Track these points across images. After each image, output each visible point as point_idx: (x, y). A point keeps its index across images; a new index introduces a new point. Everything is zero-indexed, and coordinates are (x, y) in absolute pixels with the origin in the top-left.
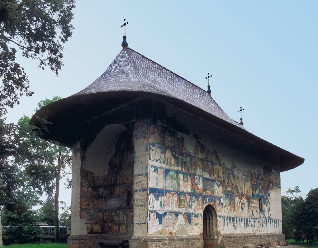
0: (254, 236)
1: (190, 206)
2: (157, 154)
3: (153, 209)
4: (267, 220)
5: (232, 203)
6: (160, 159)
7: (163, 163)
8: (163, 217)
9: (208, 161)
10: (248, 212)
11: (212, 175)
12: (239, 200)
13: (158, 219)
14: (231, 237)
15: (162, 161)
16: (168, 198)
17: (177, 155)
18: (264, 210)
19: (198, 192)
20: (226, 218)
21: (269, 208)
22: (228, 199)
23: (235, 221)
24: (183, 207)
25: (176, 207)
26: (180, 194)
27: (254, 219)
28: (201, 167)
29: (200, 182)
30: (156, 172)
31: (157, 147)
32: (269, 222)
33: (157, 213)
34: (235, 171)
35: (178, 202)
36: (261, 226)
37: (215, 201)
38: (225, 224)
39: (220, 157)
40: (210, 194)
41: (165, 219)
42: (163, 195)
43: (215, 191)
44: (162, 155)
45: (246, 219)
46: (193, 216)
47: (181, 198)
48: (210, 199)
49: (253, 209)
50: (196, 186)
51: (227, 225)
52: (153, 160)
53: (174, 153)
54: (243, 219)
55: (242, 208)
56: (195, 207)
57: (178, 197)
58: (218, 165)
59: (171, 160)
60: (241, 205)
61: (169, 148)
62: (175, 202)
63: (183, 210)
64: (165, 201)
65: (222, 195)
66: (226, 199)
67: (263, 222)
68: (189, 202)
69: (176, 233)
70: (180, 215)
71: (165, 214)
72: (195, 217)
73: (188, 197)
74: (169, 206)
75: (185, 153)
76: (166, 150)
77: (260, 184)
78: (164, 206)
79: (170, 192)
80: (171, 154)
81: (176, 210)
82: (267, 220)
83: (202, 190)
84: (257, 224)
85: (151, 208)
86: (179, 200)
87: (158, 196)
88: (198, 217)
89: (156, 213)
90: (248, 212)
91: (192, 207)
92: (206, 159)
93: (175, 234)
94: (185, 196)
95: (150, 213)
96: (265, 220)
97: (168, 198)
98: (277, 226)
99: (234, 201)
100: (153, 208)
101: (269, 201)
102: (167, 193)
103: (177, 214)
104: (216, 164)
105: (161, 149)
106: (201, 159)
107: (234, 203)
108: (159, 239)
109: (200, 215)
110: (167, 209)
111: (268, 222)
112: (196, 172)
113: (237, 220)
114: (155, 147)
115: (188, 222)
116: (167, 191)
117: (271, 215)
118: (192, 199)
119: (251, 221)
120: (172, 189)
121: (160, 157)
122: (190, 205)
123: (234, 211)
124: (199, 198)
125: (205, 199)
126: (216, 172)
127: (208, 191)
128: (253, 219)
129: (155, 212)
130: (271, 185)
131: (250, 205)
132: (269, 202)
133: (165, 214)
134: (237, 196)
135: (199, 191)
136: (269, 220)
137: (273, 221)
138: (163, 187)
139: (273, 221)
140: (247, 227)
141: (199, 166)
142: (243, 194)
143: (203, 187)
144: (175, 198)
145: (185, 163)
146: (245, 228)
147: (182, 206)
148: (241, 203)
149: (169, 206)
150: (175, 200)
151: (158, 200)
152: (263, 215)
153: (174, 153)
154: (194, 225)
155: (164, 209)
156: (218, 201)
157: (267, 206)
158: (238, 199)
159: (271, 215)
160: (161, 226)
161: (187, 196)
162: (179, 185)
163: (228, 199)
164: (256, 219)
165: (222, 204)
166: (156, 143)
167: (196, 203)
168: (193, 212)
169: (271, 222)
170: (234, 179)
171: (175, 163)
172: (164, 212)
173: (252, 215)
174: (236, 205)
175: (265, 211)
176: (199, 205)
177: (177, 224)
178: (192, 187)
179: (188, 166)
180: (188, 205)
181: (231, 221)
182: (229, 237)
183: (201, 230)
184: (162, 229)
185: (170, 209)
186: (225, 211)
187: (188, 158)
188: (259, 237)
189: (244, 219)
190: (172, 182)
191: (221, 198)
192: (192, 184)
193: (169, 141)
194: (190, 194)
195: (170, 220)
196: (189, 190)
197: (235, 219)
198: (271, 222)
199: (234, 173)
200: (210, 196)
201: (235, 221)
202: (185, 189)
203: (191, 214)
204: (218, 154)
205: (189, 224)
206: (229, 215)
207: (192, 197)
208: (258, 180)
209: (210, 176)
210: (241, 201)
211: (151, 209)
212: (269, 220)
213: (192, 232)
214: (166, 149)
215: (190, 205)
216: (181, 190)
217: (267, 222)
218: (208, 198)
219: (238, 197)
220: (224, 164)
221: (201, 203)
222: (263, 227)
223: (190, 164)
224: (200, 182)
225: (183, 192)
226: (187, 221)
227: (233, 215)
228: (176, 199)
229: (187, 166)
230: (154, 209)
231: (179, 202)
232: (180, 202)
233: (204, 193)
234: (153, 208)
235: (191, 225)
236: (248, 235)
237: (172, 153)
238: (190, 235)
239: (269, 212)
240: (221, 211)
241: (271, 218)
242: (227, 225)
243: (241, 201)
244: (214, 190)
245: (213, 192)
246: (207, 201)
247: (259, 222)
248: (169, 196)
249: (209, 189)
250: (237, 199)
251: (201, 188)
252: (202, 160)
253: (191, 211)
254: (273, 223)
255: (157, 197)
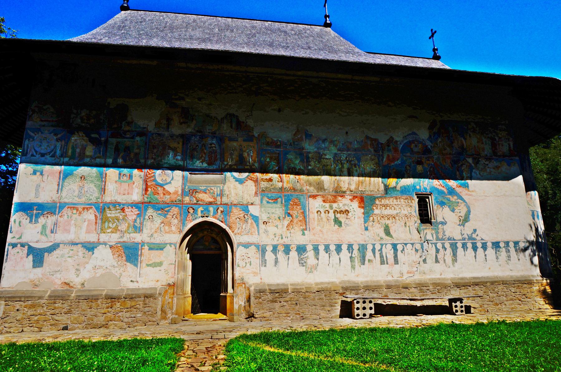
0: (389, 287)
1: (139, 229)
2: (45, 145)
3: (19, 241)
4: (459, 245)
5: (294, 213)
6: (52, 151)
7: (62, 156)
8: (46, 254)
9: (203, 137)
10: (366, 229)
11: (218, 162)
12: (327, 205)
13: (31, 257)
14: (285, 291)
15: (58, 153)
16: (66, 217)
17: (103, 139)
18: (439, 219)
19: (167, 198)
20: (269, 248)
21: (463, 214)
22: (279, 205)
23: (310, 254)
24: (112, 232)
25: (88, 232)
26: (102, 209)
27: (394, 246)
28: (180, 150)
29: (173, 178)
30: (38, 173)
31: (46, 132)
32: (470, 250)
33: (30, 247)
34: (309, 147)
35: (96, 223)
36: (431, 260)
37: (226, 213)
38: (264, 263)
39: (250, 123)
40: (212, 200)
41: (48, 258)
42: (53, 213)
43: (227, 192)
44: (59, 144)
45: (356, 247)
46: (146, 247)
47: (109, 215)
48: (209, 211)
49: (388, 222)
50: (159, 189)
51: (276, 262)
52: (32, 155)
53: (93, 136)
54: (344, 247)
55: (340, 223)
56: (153, 231)
57: (97, 214)
58: (240, 139)
59: (84, 148)
60: (331, 215)
61: (79, 129)
62: (86, 223)
63: (114, 238)
64: (55, 224)
65: (257, 200)
66: (269, 205)
67: (437, 251)
68: (135, 221)
69: (83, 284)
70: (101, 247)
71: (55, 247)
72: (150, 249)
73: (132, 214)
74: (68, 231)
75: (129, 131)
76: (74, 134)
77: (420, 163)
78: (52, 232)
79: (73, 207)
80: (85, 138)
81: (92, 238)
82: (459, 245)
83: (180, 192)
84: (408, 257)
85: (14, 237)
86: (102, 219)
87: (37, 216)
88: (162, 249)
89: (27, 247)
90: (366, 229)
91: (145, 230)
92: (199, 134)
93: (79, 287)
94: (123, 210)
95: (11, 247)
96: (447, 245)
97: (66, 217)
98: (509, 257)
99: (304, 208)
100: (20, 238)
101: (464, 197)
102: (66, 208)
103: (90, 247)
104: (231, 139)
105: (56, 135)
106: (182, 136)
107: (303, 213)
108: (20, 297)
109: (170, 244)
110: (59, 237)
111: (464, 246)
112: (161, 161)
113: (316, 249)
114: (42, 133)
115: (129, 260)
116: (62, 206)
117: (475, 231)
118: (145, 214)
119: (381, 250)
120: (83, 200)
121: (53, 147)
122: (134, 227)
123: (306, 229)
124: (168, 211)
125: (191, 211)
126: (231, 154)
127: (201, 196)
128: (390, 247)
129: (23, 245)
130: (470, 160)
131: (376, 211)
132: (462, 199)
133: (55, 247)
134: (314, 197)
135: (168, 197)
136: (469, 245)
137: (489, 245)
138: (54, 198)
139: (489, 245)
140: (364, 264)
141: (174, 150)
142: (344, 189)
143: (183, 190)
144: (90, 215)
145: (127, 149)
146: (353, 267)
147: (109, 230)
148: (331, 212)
149: (68, 231)
150: (89, 221)
151: (36, 222)
152: (437, 233)
153: (93, 136)
154: (148, 265)
155: (52, 240)
156: (237, 212)
157: (453, 211)
158: (322, 203)
159: (475, 231)
160: (39, 270)
161: (126, 210)
162: (103, 190)
163: (279, 205)
164: (406, 244)
165: (256, 219)
166: (44, 126)
167: (159, 221)
168: (147, 240)
169: (480, 251)
170: (302, 161)
171: (95, 153)
172: (51, 244)
173: (383, 235)
174: (312, 216)
175: (444, 223)
176: (170, 224)
177: (89, 267)
178: (146, 190)
179: (137, 154)
180: (128, 227)
181: (294, 254)
182: (272, 292)
183: (170, 275)
184: (41, 276)
185: (71, 237)
186: (266, 231)
187: (138, 138)
188: (413, 290)
189: (350, 247)
190: (82, 187)
191: (252, 204)
192: (147, 184)
193: (82, 118)
194: (134, 205)
195: (69, 259)
196: (136, 195)
197: (309, 248)
198: (480, 251)
199: (303, 149)
200: (211, 203)
201: (310, 254)
202: (125, 197)
203: (138, 244)
204: (242, 118)
205: (128, 264)
206: (287, 241)
207: (146, 210)
208: (409, 154)
209: (209, 164)
210: (331, 207)
211: (14, 241)
212: (474, 244)
213: (137, 282)
214: (72, 133)
215: (134, 227)
216: (107, 199)
217: (460, 251)
218: (201, 209)
219: (319, 200)
220: (263, 135)
221: (176, 221)
222: (437, 261)
223: (142, 149)
224: (173, 178)
225: (115, 204)
226: (124, 258)
227: (297, 238)
228: (94, 218)
229: (132, 155)
230: (23, 240)
231: (99, 221)
232: (103, 222)
233: (187, 199)
234: (20, 238)
235: (136, 265)
236: (362, 286)
237: (88, 135)
238: (131, 287)
239: (467, 224)
240: (249, 233)
241: (475, 239)
242: (276, 262)
243: (331, 207)
244: (222, 191)
245: (221, 195)
246: (200, 214)
247: (417, 251)
248: (70, 214)
249: (206, 189)
250: (316, 204)
251: (176, 193)
252: (185, 139)
253: (138, 238)
254: (490, 251)
255: (34, 219)
